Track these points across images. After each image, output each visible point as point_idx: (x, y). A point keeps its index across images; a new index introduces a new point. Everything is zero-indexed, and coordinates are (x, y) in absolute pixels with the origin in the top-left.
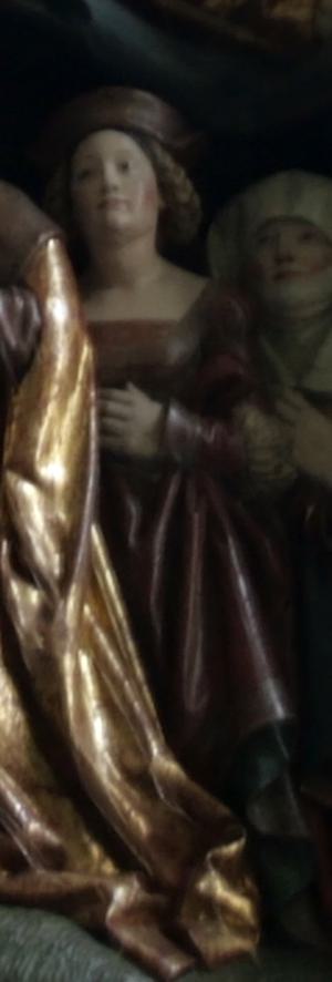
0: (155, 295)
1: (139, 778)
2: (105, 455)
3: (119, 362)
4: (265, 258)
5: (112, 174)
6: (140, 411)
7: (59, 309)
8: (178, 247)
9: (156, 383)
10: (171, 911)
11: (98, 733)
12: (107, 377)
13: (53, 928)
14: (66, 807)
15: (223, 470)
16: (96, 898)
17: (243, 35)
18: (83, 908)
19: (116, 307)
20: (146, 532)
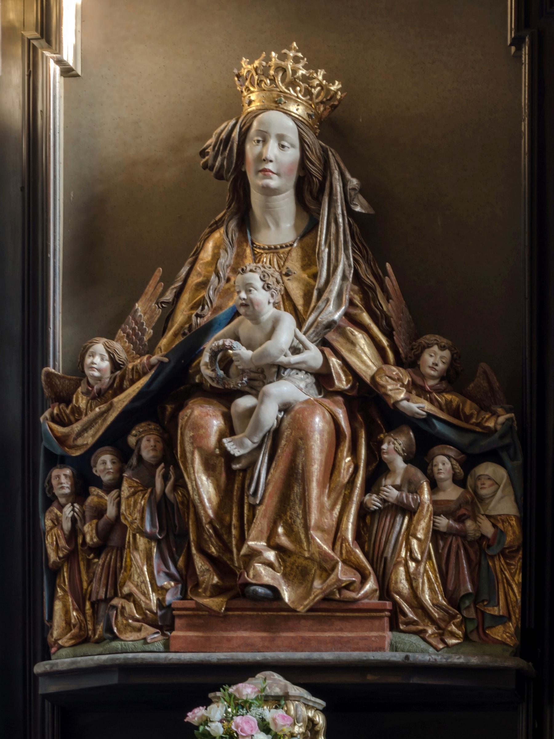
0: (451, 493)
1: (437, 605)
2: (433, 530)
3: (440, 508)
4: (479, 484)
5: (441, 466)
6: (443, 522)
7: (426, 496)
8: (459, 481)
9: (447, 515)
10: (441, 635)
11: (427, 597)
12: (436, 513)
13: (415, 639)
14: (420, 611)
15: (462, 535)
16: (425, 631)
17: (478, 429)
18: (421, 633)
19: (441, 496)
20: (443, 548)
